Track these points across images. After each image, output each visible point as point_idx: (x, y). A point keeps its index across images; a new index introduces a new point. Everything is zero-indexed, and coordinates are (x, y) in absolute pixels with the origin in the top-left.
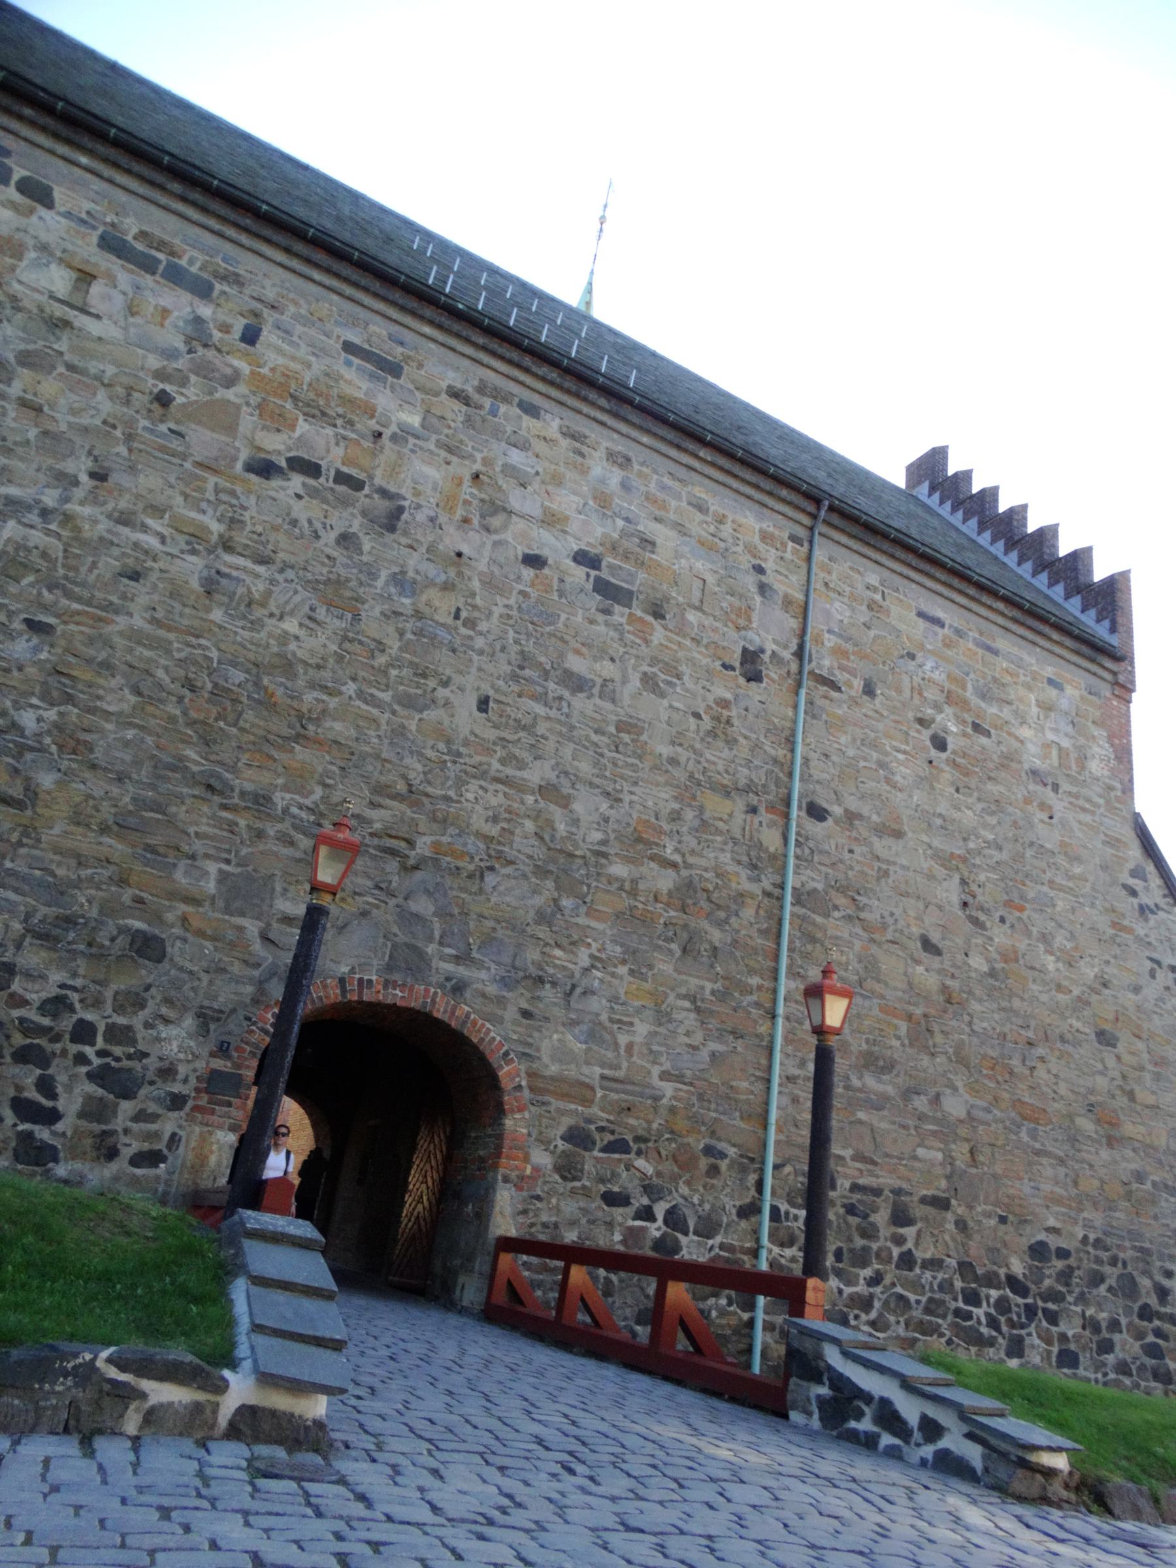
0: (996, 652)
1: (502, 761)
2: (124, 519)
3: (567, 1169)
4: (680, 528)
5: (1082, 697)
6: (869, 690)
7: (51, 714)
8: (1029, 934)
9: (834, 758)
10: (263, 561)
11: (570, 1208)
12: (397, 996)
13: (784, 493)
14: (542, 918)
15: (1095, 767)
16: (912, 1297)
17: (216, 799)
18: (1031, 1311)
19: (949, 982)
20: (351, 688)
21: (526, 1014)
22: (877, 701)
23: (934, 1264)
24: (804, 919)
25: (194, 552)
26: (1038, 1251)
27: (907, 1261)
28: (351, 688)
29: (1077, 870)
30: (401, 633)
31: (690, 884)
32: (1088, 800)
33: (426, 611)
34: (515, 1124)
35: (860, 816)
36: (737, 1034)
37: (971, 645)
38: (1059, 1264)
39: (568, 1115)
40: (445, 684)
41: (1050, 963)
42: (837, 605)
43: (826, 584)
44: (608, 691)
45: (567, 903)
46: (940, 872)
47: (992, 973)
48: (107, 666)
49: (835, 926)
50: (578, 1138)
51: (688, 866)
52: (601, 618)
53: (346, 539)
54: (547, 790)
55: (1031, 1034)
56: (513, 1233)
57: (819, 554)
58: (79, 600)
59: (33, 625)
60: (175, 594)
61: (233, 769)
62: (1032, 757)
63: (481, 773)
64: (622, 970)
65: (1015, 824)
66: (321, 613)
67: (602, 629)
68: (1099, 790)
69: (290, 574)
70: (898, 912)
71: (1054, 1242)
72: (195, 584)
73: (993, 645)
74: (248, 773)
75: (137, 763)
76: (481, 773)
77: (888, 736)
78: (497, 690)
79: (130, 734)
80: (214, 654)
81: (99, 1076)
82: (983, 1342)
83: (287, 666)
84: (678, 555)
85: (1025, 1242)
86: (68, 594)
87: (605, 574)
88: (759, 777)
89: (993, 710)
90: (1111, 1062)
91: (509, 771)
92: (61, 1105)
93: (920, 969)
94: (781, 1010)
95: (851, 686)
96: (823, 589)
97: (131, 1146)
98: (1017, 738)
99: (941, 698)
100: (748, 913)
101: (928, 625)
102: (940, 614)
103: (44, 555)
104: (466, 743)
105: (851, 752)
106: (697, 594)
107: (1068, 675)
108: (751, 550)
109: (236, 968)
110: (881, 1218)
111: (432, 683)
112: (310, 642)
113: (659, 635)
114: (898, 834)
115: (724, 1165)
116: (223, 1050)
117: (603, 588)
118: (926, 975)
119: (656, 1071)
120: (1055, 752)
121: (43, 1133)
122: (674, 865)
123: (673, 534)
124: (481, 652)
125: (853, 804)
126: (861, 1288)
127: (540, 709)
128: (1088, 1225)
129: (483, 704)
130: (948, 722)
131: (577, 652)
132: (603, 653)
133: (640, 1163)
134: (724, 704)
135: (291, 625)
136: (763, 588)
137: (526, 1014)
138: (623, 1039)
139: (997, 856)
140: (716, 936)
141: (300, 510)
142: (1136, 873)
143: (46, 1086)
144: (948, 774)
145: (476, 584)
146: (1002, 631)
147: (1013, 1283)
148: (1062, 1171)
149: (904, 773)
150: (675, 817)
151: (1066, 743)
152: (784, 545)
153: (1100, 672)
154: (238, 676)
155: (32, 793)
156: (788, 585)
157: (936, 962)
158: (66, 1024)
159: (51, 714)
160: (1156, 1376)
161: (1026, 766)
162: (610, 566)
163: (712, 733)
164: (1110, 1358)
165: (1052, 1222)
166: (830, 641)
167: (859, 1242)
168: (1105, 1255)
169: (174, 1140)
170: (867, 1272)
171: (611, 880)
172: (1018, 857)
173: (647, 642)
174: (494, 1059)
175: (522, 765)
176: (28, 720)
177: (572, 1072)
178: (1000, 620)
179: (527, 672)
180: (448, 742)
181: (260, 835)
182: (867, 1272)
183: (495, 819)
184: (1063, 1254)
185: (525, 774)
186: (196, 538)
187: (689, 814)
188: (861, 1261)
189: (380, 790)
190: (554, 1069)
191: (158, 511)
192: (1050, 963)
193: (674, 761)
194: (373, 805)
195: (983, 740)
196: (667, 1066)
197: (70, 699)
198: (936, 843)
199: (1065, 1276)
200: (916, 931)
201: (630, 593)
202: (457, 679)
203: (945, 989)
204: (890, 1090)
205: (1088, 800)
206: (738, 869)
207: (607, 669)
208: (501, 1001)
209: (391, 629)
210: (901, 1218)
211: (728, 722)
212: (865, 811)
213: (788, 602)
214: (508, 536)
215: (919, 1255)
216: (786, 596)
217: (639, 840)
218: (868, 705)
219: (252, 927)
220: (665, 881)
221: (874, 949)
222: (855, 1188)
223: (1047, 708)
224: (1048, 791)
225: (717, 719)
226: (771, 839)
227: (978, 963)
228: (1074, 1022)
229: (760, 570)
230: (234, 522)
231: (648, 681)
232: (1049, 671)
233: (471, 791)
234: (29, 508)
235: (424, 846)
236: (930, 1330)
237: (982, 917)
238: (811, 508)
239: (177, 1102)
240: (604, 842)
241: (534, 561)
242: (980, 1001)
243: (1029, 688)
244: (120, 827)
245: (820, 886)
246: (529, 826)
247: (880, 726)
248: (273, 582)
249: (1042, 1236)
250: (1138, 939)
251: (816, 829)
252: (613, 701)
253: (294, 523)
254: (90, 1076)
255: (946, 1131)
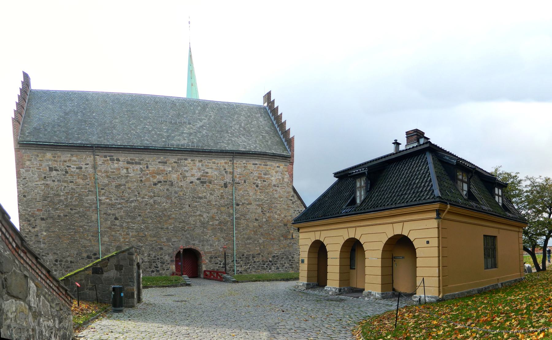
0: (267, 165)
1: (193, 213)
2: (143, 198)
3: (210, 261)
4: (212, 168)
5: (284, 167)
6: (245, 182)
7: (144, 225)
8: (273, 213)
9: (240, 195)
10: (159, 197)
11: (211, 265)
12: (188, 247)
13: (227, 154)
14: (202, 233)
15: (286, 180)
16: (255, 266)
17: (163, 230)
18: (272, 264)
19: (260, 224)
20: (173, 210)
21: (202, 245)
22: (246, 183)
23: (259, 262)
24: (237, 221)
25: (151, 199)
26: (274, 257)
27: (255, 262)
28: (173, 210)
29: (281, 200)
30: (177, 200)
31: (220, 222)
32: (284, 186)
33: (179, 195)
34: (203, 258)
35: (245, 203)
36: (229, 240)
37: (262, 166)
38: (277, 258)
39: (209, 255)
40: (184, 205)
41: (276, 216)
42: (238, 169)
43: (236, 167)
44: (205, 197)
45: (205, 230)
46: (258, 207)
47: (267, 221)
48: (147, 217)
49: (242, 221)
50: (211, 258)
51: (220, 219)
52: (202, 187)
53: (167, 190)
54: (200, 215)
55: (273, 228)
56: (205, 269)
57: (235, 162)
58: (142, 210)
59: (139, 215)
60: (151, 205)
61: (164, 226)
62: (274, 183)
63: (191, 216)
64: (213, 236)
65: (270, 196)
66: (167, 201)
67: (203, 188)
68: (286, 184)
69: (162, 197)
70: (251, 216)
71: (276, 255)
72: (153, 203)
73: (266, 164)
74: (165, 225)
75: (154, 228)
76: (191, 216)
77: (248, 188)
78: (191, 203)
79: (152, 225)
80: (157, 212)
81: (161, 263)
82: (265, 269)
83: (165, 210)
84: (212, 173)
85: (272, 256)
86: (141, 210)
87: (202, 180)
88: (228, 202)
89: (267, 176)
90: (286, 228)
91: (194, 214)
92: (158, 266)
93: (255, 224)
94: (235, 236)
95: (242, 182)
96: (236, 168)
97: (166, 269)
98: (271, 180)
99: (257, 178)
100: (229, 223)
101: (255, 166)
102: (257, 162)
103: (137, 206)
104: (188, 212)
105: (242, 193)
106: (216, 177)
107: (281, 164)
108: (223, 166)
109: (170, 248)
110: (251, 258)
111: (182, 205)
112: (167, 205)
113: (211, 186)
114: (251, 204)
115: (229, 257)
116: (171, 257)
117: (202, 182)
118: (256, 224)
119: (219, 248)
120: (278, 180)
121: (158, 269)
122: (218, 220)
123: (211, 170)
124: (187, 199)
125: (243, 201)
126: (248, 267)
127: (197, 204)
128: (281, 251)
129: (189, 206)
130: (259, 182)
131: (200, 193)
132: (204, 192)
133: (219, 259)
134: (222, 193)
135: (164, 204)
136: (226, 172)
137: (202, 245)
138: (214, 245)
139: (267, 202)
140: (225, 228)
141: (161, 188)
142: (293, 196)
143: (157, 265)
144: (259, 191)
145: (185, 189)
146: (268, 161)
147: (270, 261)
148: (277, 246)
149: (251, 194)
150: (217, 213)
151: (280, 177)
152: (229, 163)
153: (287, 161)
154: (161, 213)
155: (145, 235)
156: (230, 170)
157: (258, 222)
158: (156, 258)
159: (144, 225)
160: (291, 268)
161: (273, 185)
162: (202, 179)
163: (221, 198)
164: (284, 267)
165: (276, 252)
166: (238, 176)
167: (248, 261)
168: (284, 255)
169: (169, 267)
170: (249, 265)
171: (210, 225)
172: (271, 201)
173: (209, 188)
174: (200, 251)
175: (196, 213)
176: (142, 227)
177: (209, 251)
178: (268, 159)
179: (194, 199)
180: (186, 213)
181: (168, 233)
182: (249, 265)
183: (194, 222)
184: (277, 256)
185: (196, 214)
186: (151, 197)
187: (219, 212)
188: (248, 263)
189: (180, 222)
190: (207, 251)
191: (146, 195)
192: (276, 216)
193: (216, 205)
194: (179, 224)
195: (265, 183)
196: (220, 247)
197: (145, 223)
198: (257, 203)
199: (278, 259)
200: (254, 218)
201: (206, 182)
202: (185, 203)
203: (259, 225)
204: (251, 242)
205: (284, 186)
206: (227, 217)
207: (204, 194)
208: (199, 244)
209: (176, 200)
210: (253, 257)
211: (223, 196)
212: (245, 202)
213: (230, 172)
214: (187, 180)
215: (256, 261)
216: (230, 172)
217: (213, 218)
218: (245, 185)
219: (170, 244)
220: (217, 222)
221: (248, 223)
222: (247, 255)
223: (276, 172)
224: (277, 187)
225: (221, 196)
226: (231, 211)
227: (264, 220)
228: (280, 224)
229: (225, 169)
230: (154, 193)
231: (211, 194)
232: (277, 165)
233: (190, 219)
234: (133, 201)
235: (186, 228)
236: (259, 269)
237: (265, 212)
238: (232, 154)
239: (168, 264)
240: (208, 220)
241: (192, 182)
242: (265, 225)
243: (273, 170)
244: (155, 237)
245: (239, 216)
246: (198, 221)
247: (247, 187)
248: (161, 199)
249: (274, 255)
250: (292, 208)
251: (238, 207)
252: (206, 199)
253: (161, 190)
254: (160, 263)
255: (260, 244)
